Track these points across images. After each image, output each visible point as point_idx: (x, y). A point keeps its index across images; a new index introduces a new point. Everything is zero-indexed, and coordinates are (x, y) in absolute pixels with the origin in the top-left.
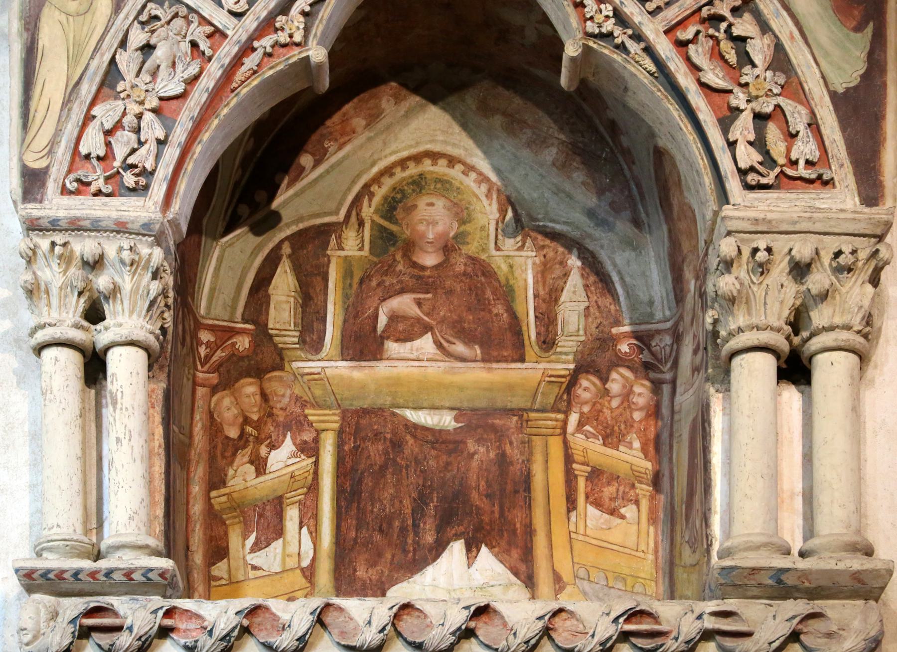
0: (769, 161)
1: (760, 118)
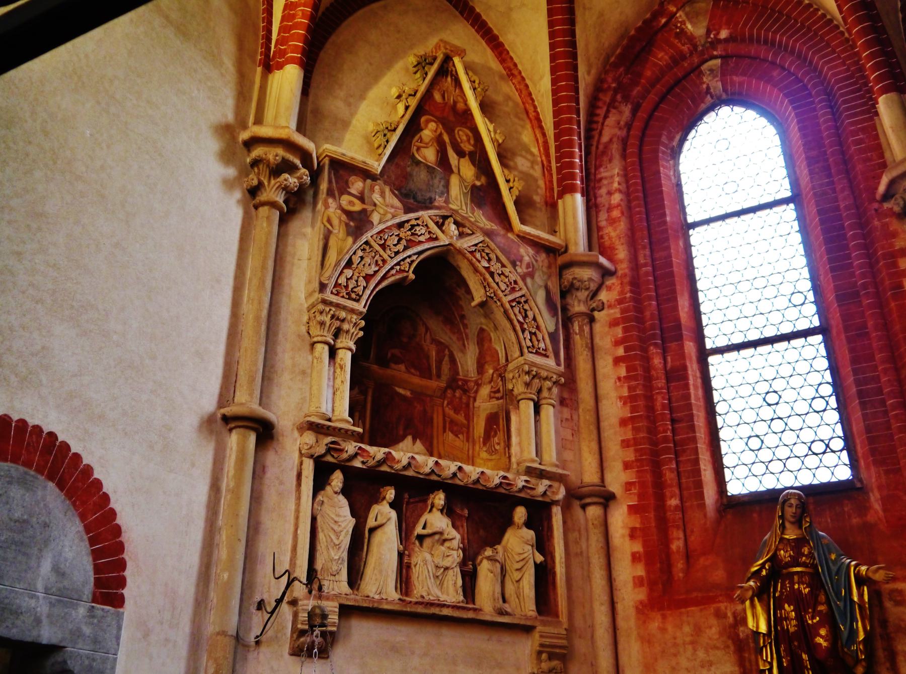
0: (533, 346)
1: (530, 333)
